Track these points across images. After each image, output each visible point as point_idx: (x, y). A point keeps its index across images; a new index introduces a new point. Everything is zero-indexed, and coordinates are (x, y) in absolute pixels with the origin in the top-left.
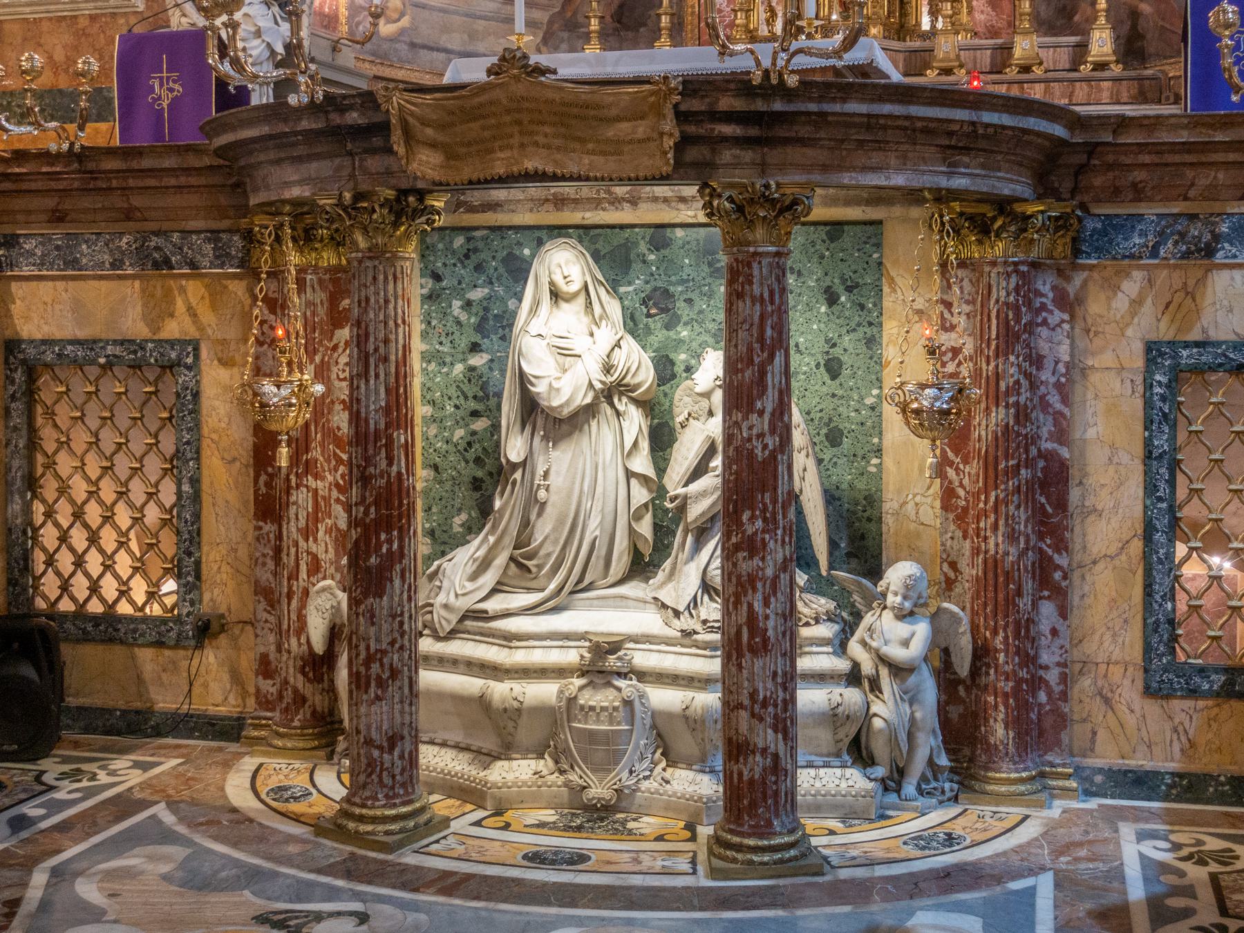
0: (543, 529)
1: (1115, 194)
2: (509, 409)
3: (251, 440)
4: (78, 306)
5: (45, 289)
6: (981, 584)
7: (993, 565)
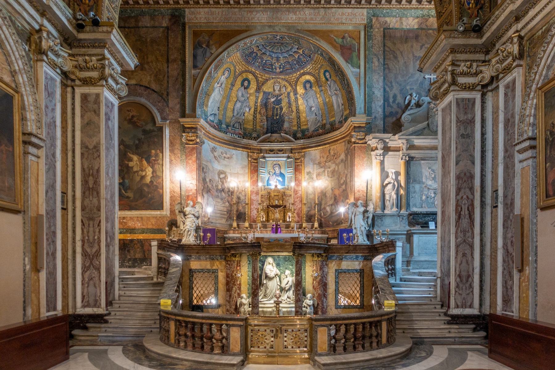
0: (268, 291)
1: (332, 253)
2: (263, 277)
3: (225, 282)
4: (200, 265)
5: (195, 262)
6: (318, 296)
7: (319, 294)
